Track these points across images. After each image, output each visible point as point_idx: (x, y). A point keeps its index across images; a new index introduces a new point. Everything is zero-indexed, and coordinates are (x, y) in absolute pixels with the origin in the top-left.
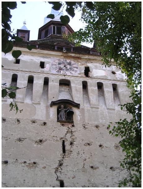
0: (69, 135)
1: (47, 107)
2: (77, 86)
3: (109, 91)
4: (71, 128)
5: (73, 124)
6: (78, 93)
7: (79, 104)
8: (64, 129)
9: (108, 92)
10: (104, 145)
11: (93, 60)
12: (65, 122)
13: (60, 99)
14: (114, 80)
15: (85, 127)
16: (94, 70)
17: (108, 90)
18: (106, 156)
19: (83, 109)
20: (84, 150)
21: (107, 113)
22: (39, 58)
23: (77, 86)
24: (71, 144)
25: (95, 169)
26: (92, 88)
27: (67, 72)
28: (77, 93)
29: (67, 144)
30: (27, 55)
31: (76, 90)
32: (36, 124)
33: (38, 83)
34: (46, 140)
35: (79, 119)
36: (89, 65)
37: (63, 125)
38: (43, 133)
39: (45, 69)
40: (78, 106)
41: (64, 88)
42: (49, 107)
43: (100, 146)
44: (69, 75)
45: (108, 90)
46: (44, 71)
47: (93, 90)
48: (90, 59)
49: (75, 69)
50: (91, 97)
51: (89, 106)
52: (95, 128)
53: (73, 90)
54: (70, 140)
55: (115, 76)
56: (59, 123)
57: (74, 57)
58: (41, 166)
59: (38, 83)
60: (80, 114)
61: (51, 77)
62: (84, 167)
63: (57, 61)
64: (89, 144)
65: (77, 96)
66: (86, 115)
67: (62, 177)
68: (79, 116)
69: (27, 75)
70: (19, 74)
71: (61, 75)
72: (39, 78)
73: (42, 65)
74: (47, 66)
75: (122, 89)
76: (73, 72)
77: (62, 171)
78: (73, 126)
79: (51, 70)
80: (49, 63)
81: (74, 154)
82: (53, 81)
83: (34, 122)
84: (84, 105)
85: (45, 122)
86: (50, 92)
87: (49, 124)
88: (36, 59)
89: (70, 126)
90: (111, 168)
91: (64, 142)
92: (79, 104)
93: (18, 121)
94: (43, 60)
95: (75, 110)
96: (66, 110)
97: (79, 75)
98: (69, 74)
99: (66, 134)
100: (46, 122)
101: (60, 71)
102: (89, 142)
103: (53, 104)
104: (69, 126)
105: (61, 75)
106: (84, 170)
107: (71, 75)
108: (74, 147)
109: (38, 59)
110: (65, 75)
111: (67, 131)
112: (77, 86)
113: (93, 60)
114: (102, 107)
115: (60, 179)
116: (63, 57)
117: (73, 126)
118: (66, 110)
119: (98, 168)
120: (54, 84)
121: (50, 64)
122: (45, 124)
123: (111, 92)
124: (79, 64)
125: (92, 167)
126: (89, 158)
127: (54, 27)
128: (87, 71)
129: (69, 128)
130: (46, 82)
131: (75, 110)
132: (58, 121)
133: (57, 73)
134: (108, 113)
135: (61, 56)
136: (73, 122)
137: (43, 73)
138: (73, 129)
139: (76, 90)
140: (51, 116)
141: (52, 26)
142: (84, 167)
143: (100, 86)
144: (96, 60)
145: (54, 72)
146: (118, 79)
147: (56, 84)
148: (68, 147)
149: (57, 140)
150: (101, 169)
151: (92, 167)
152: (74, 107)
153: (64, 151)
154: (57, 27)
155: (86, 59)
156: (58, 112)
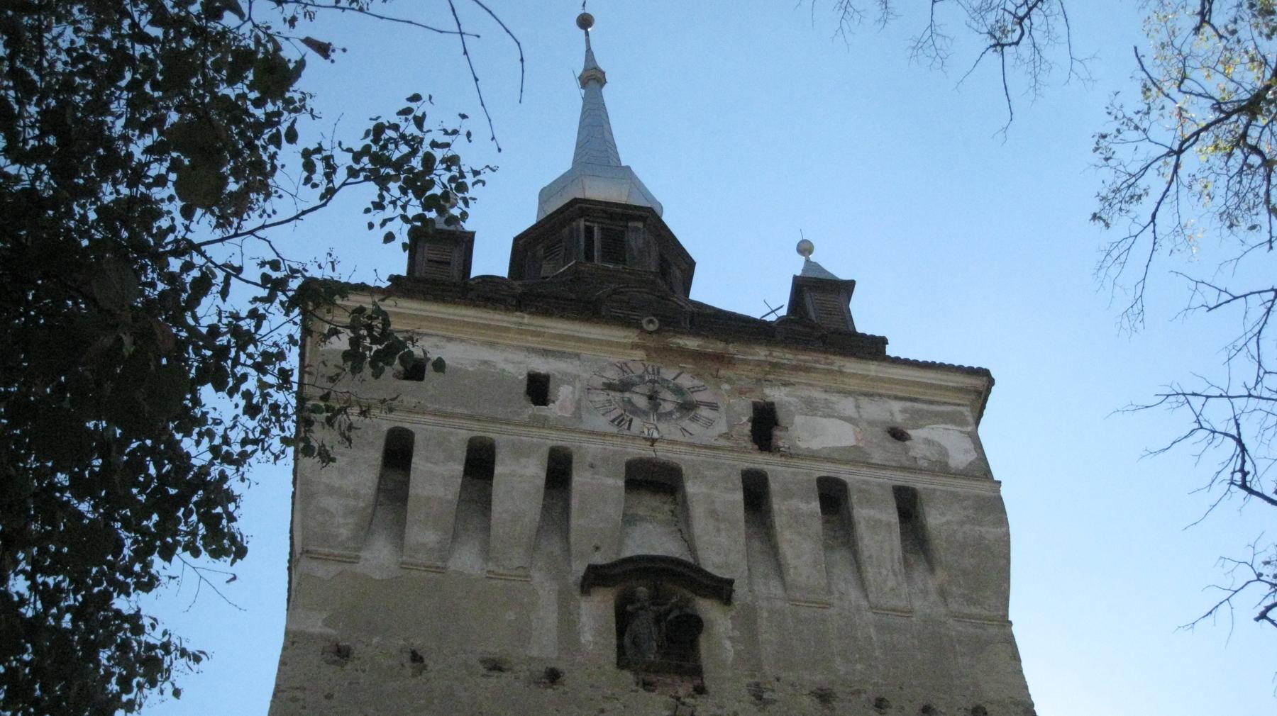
1: (563, 600)
2: (716, 493)
3: (880, 521)
4: (689, 700)
5: (697, 682)
6: (723, 526)
7: (731, 582)
9: (876, 525)
13: (627, 553)
14: (903, 468)
15: (761, 698)
16: (799, 420)
17: (875, 521)
21: (872, 631)
22: (520, 356)
26: (795, 510)
27: (661, 426)
28: (719, 530)
31: (713, 514)
32: (506, 677)
33: (520, 476)
35: (732, 653)
36: (776, 394)
37: (648, 686)
40: (721, 590)
41: (648, 503)
42: (577, 593)
44: (670, 440)
45: (875, 521)
46: (546, 418)
47: (796, 517)
48: (775, 366)
49: (704, 412)
50: (786, 549)
51: (779, 592)
53: (698, 512)
55: (906, 450)
56: (628, 676)
57: (698, 356)
59: (520, 476)
60: (737, 633)
61: (586, 449)
65: (719, 544)
66: (768, 635)
68: (728, 644)
69: (460, 436)
70: (423, 428)
71: (634, 438)
72: (520, 452)
73: (538, 389)
74: (564, 395)
75: (942, 514)
76: (694, 427)
78: (700, 690)
79: (585, 415)
80: (570, 379)
82: (592, 466)
84: (759, 590)
85: (553, 666)
86: (576, 521)
88: (506, 360)
89: (684, 689)
92: (731, 582)
93: (416, 658)
94: (541, 366)
95: (707, 608)
97: (722, 442)
100: (561, 666)
101: (631, 421)
103: (595, 578)
104: (681, 692)
105: (634, 438)
107: (687, 439)
113: (796, 368)
117: (700, 690)
120: (598, 489)
121: (578, 385)
122: (553, 676)
123: (889, 525)
127: (589, 231)
128: (765, 425)
129: (678, 699)
130: (559, 471)
131: (707, 608)
132: (622, 663)
133: (614, 430)
135: (635, 346)
136: (697, 671)
137: (543, 423)
139: (713, 514)
140: (587, 637)
143: (833, 496)
144: (807, 370)
145: (601, 422)
147: (610, 481)
152: (705, 596)
154: (602, 229)
155: (759, 364)
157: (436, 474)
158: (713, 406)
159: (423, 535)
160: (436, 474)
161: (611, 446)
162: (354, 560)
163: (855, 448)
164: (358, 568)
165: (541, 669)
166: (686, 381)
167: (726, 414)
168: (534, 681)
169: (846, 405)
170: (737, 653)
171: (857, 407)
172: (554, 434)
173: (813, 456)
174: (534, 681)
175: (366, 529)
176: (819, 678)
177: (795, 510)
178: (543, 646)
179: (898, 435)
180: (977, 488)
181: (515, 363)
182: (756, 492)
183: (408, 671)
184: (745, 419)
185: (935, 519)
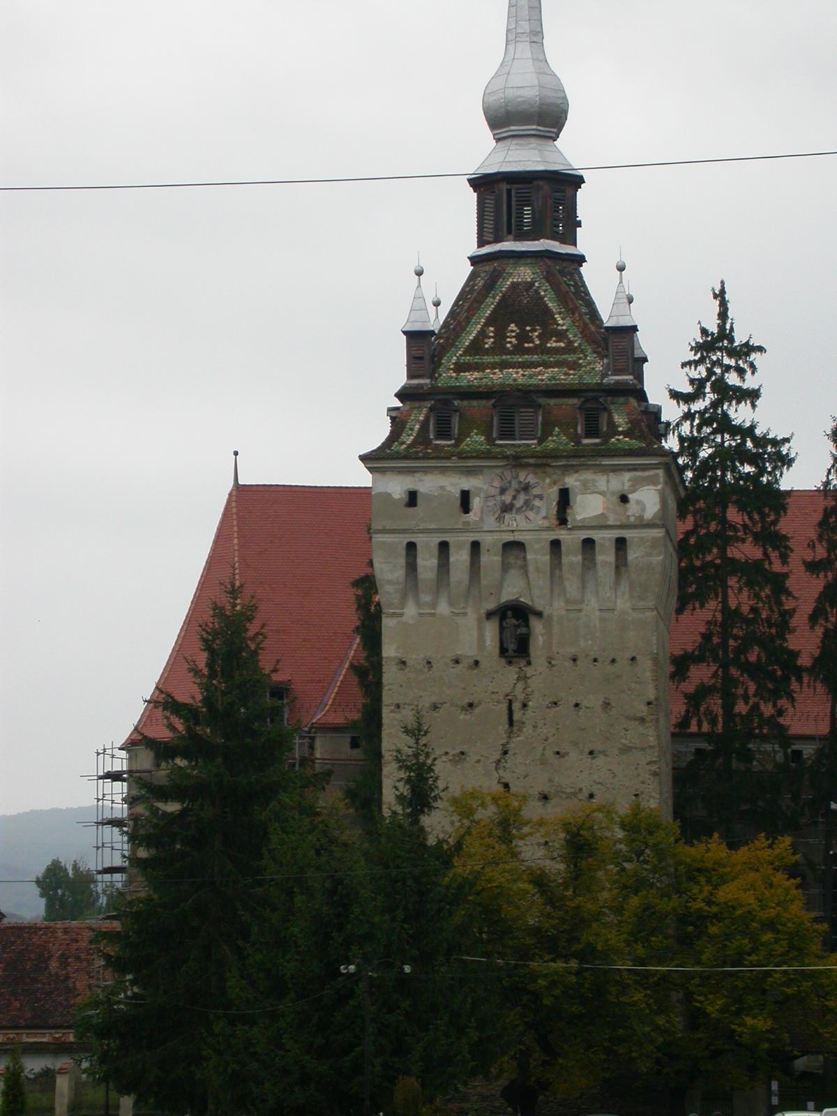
0: (520, 685)
1: (479, 621)
3: (606, 562)
4: (523, 668)
8: (512, 673)
9: (605, 563)
10: (584, 703)
11: (580, 465)
12: (514, 657)
13: (503, 600)
15: (550, 663)
16: (579, 498)
18: (584, 729)
19: (550, 617)
20: (545, 719)
21: (597, 622)
24: (525, 705)
25: (563, 757)
26: (572, 558)
29: (516, 706)
30: (431, 473)
32: (461, 666)
33: (459, 558)
34: (479, 703)
36: (571, 481)
37: (510, 663)
38: (475, 686)
39: (473, 516)
40: (539, 614)
42: (484, 619)
43: (577, 705)
45: (606, 556)
46: (468, 523)
51: (562, 604)
52: (568, 664)
53: (531, 568)
54: (521, 697)
55: (626, 510)
56: (503, 660)
57: (535, 465)
58: (472, 758)
59: (459, 558)
61: (486, 540)
62: (543, 755)
63: (497, 483)
64: (556, 703)
67: (507, 777)
69: (436, 539)
70: (419, 539)
73: (465, 497)
74: (476, 503)
75: (635, 553)
76: (531, 515)
77: (507, 765)
81: (528, 730)
82: (488, 551)
83: (457, 662)
84: (555, 608)
87: (485, 664)
88: (452, 484)
89: (523, 663)
90: (591, 753)
91: (510, 703)
93: (429, 663)
96: (515, 623)
98: (523, 524)
99: (515, 684)
100: (478, 659)
101: (504, 517)
102: (555, 700)
103: (489, 615)
106: (543, 762)
108: (529, 713)
109: (454, 484)
110: (513, 531)
111: (516, 676)
112: (538, 557)
113: (580, 465)
114: (592, 604)
115: (503, 780)
116: (509, 467)
117: (529, 663)
118: (515, 623)
119: (567, 754)
120: (491, 559)
121: (482, 496)
124: (548, 481)
125: (558, 753)
126: (554, 735)
127: (509, 191)
128: (565, 498)
132: (503, 651)
134: (602, 620)
138: (529, 671)
140: (488, 642)
141: (504, 187)
142: (543, 755)
146: (632, 519)
147: (495, 558)
148: (516, 717)
149: (499, 702)
150: (573, 755)
151: (558, 753)
153: (511, 722)
156: (502, 629)
157: (427, 563)
158: (540, 497)
160: (427, 563)
161: (496, 536)
162: (401, 615)
163: (602, 514)
164: (404, 619)
165: (471, 661)
168: (470, 667)
169: (601, 481)
170: (544, 641)
171: (608, 482)
172: (472, 534)
174: (470, 667)
175: (404, 598)
176: (572, 650)
177: (572, 558)
179: (624, 499)
182: (556, 544)
183: (426, 670)
184: (555, 503)
185: (633, 555)
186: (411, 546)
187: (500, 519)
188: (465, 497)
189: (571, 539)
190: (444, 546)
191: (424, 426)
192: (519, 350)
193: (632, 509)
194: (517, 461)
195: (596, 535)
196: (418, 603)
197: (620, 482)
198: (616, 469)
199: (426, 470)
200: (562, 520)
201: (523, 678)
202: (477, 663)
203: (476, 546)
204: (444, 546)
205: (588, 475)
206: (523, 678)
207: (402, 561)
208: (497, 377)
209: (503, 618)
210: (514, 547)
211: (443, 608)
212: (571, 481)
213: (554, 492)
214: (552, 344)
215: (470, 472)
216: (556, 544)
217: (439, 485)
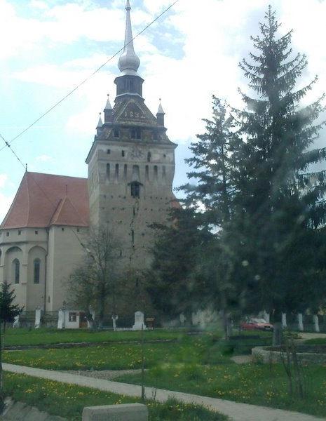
17: (160, 171)
23: (142, 170)
26: (151, 170)
29: (136, 209)
33: (121, 169)
36: (151, 150)
39: (125, 157)
40: (142, 185)
61: (128, 163)
66: (146, 189)
69: (116, 163)
70: (111, 163)
73: (123, 152)
74: (126, 154)
81: (139, 216)
96: (135, 187)
103: (129, 184)
109: (120, 149)
112: (142, 170)
118: (135, 187)
120: (129, 169)
128: (149, 155)
130: (126, 166)
132: (132, 194)
143: (156, 168)
148: (136, 212)
156: (132, 189)
157: (113, 169)
159: (111, 179)
160: (113, 169)
166: (140, 149)
167: (145, 156)
169: (159, 151)
173: (154, 162)
177: (151, 170)
178: (123, 194)
179: (165, 156)
180: (171, 165)
181: (120, 149)
182: (147, 167)
186: (108, 165)
187: (132, 159)
188: (123, 152)
189: (151, 166)
190: (117, 166)
191: (111, 133)
192: (134, 117)
193: (167, 158)
194: (138, 144)
195: (158, 165)
196: (109, 180)
197: (163, 152)
198: (163, 148)
199: (113, 144)
200: (149, 160)
201: (137, 202)
202: (125, 197)
203: (126, 166)
204: (117, 166)
205: (155, 149)
206: (137, 202)
207: (105, 168)
208: (130, 123)
209: (132, 185)
210: (136, 167)
211: (116, 182)
212: (151, 150)
213: (146, 153)
214: (142, 117)
215: (124, 146)
216: (147, 167)
217: (116, 149)
